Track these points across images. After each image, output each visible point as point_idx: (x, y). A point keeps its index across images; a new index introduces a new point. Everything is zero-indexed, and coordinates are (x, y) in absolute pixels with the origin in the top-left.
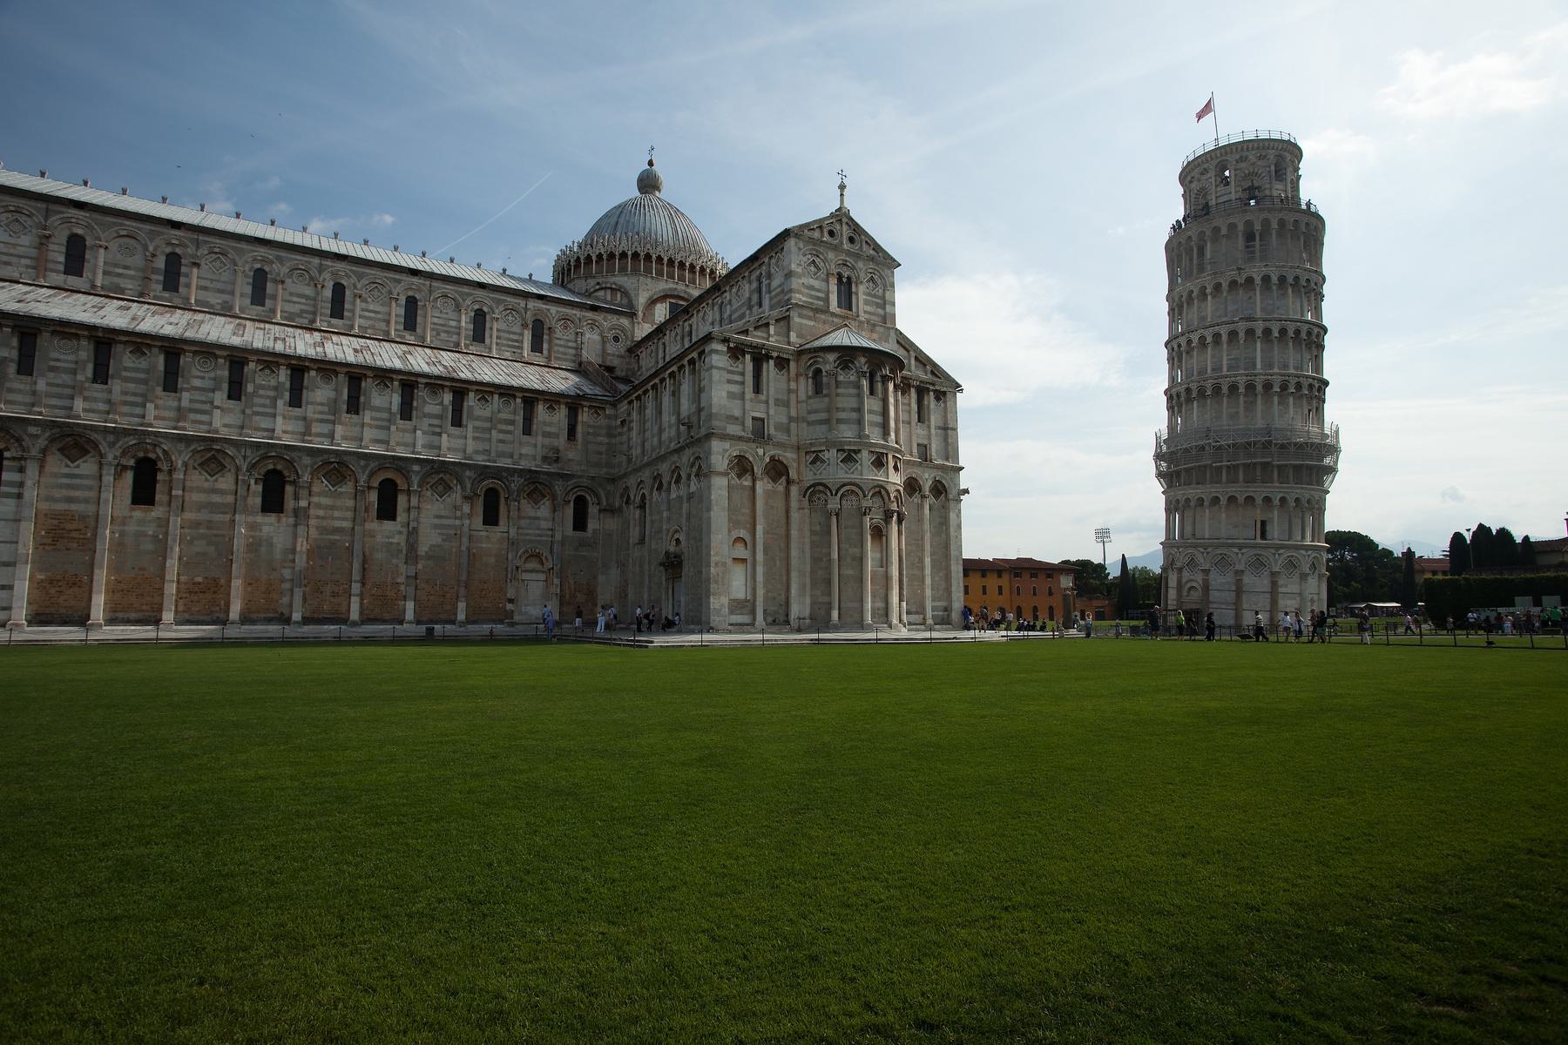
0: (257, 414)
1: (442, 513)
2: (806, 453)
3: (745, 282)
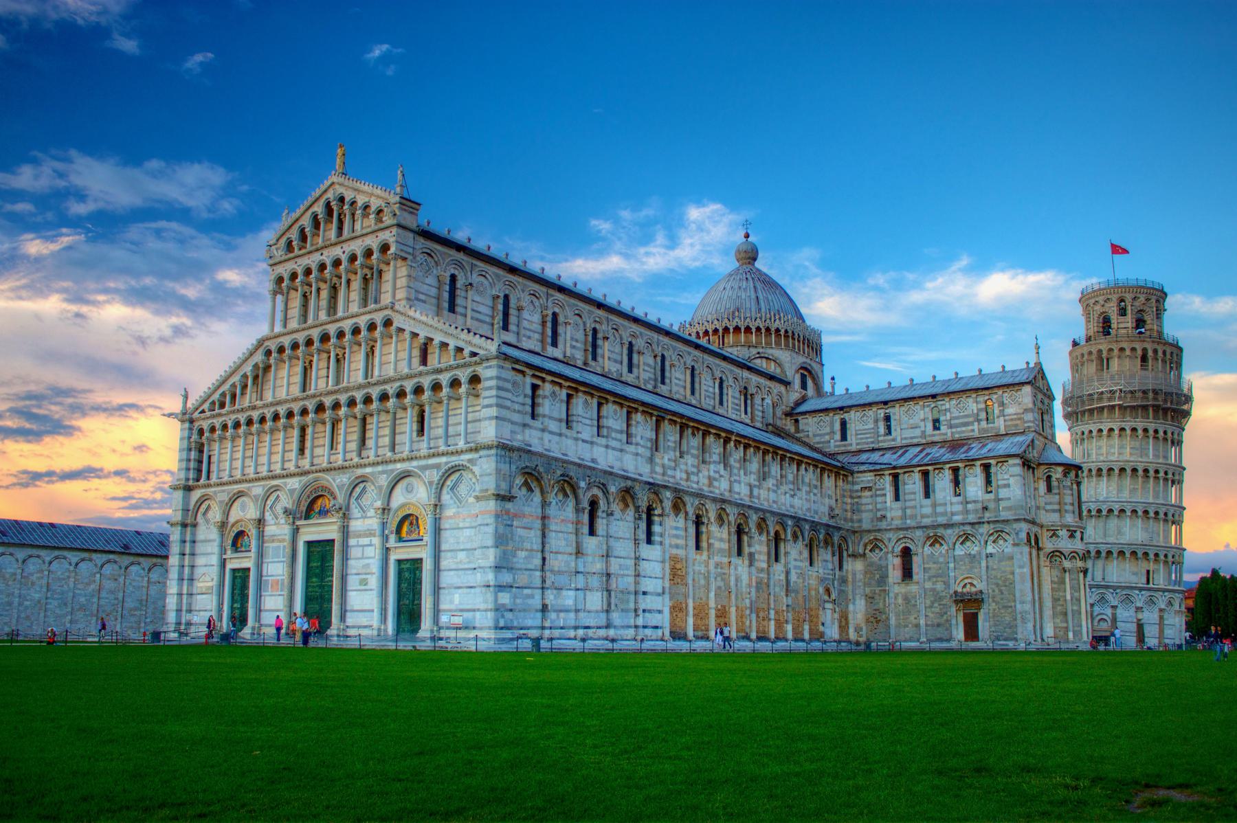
0: (735, 481)
1: (797, 557)
2: (1047, 530)
3: (970, 400)
